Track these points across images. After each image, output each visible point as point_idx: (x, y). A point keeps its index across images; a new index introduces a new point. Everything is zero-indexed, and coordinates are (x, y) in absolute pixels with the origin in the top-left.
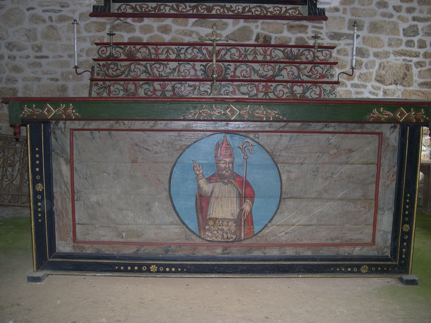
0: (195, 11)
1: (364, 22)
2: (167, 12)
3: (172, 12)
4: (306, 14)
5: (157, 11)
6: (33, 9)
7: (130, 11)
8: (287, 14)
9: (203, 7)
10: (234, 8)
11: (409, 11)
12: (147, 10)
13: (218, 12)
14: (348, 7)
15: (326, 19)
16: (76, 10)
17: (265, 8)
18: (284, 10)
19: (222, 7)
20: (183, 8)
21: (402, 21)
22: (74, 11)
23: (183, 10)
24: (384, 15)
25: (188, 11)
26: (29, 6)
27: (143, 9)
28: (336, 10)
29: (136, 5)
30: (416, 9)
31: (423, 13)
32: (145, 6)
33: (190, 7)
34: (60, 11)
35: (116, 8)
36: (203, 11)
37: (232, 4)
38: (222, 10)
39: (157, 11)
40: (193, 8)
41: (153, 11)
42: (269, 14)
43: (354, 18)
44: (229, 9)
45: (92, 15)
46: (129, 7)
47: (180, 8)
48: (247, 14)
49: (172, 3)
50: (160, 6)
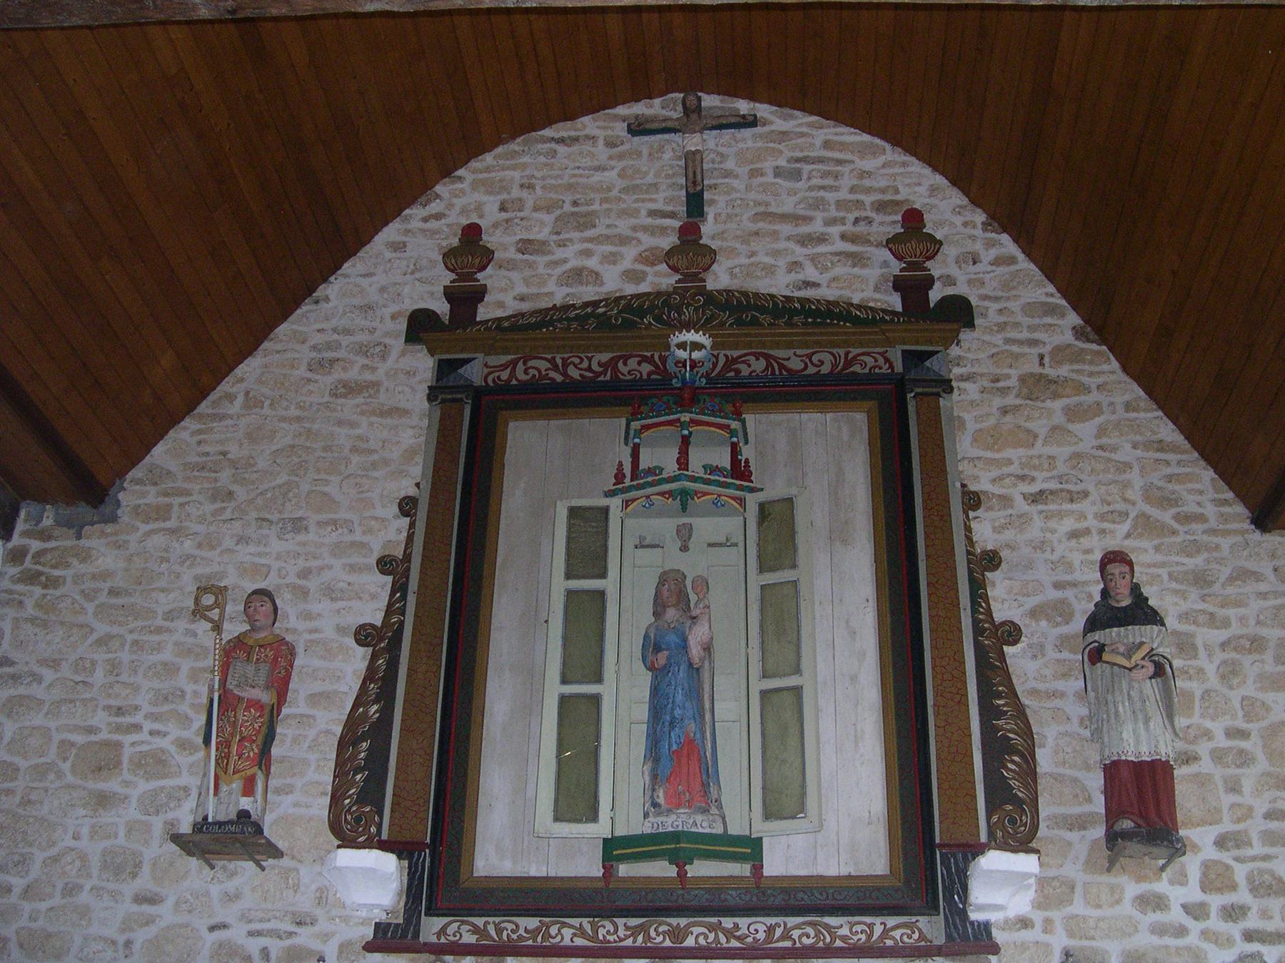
0: (640, 938)
1: (1107, 952)
2: (567, 942)
3: (579, 942)
4: (940, 940)
5: (539, 939)
6: (224, 926)
7: (469, 939)
8: (889, 943)
9: (661, 929)
10: (744, 931)
11: (1231, 916)
12: (514, 936)
13: (702, 941)
14: (1056, 915)
15: (995, 949)
16: (333, 934)
17: (828, 927)
18: (878, 930)
19: (712, 928)
20: (608, 932)
21: (1216, 942)
22: (326, 937)
23: (608, 937)
24: (1159, 930)
25: (621, 940)
26: (213, 921)
27: (505, 934)
28: (1024, 923)
29: (486, 923)
30: (1249, 908)
31: (1271, 918)
32: (511, 926)
33: (627, 928)
34: (291, 934)
35: (436, 929)
36: (660, 939)
37: (737, 920)
38: (712, 936)
39: (539, 939)
40: (635, 931)
41: (528, 939)
42: (838, 943)
43: (1072, 943)
44: (729, 934)
45: (370, 947)
46: (468, 927)
47: (602, 932)
48: (780, 944)
49: (579, 920)
50: (548, 928)
